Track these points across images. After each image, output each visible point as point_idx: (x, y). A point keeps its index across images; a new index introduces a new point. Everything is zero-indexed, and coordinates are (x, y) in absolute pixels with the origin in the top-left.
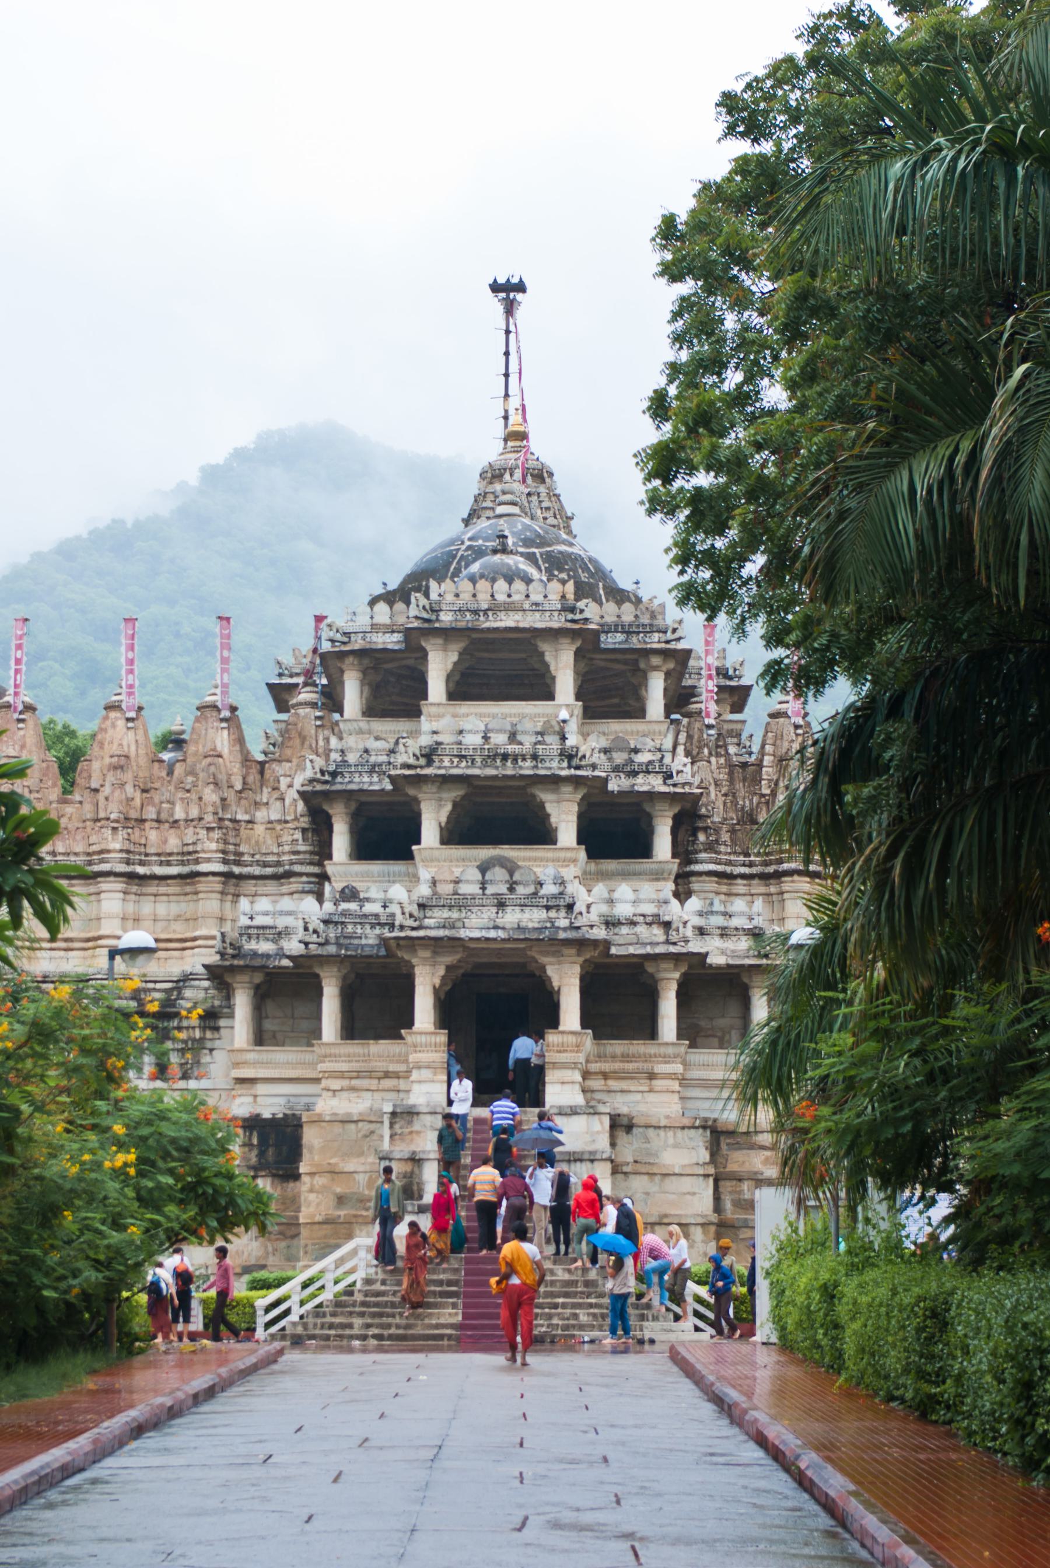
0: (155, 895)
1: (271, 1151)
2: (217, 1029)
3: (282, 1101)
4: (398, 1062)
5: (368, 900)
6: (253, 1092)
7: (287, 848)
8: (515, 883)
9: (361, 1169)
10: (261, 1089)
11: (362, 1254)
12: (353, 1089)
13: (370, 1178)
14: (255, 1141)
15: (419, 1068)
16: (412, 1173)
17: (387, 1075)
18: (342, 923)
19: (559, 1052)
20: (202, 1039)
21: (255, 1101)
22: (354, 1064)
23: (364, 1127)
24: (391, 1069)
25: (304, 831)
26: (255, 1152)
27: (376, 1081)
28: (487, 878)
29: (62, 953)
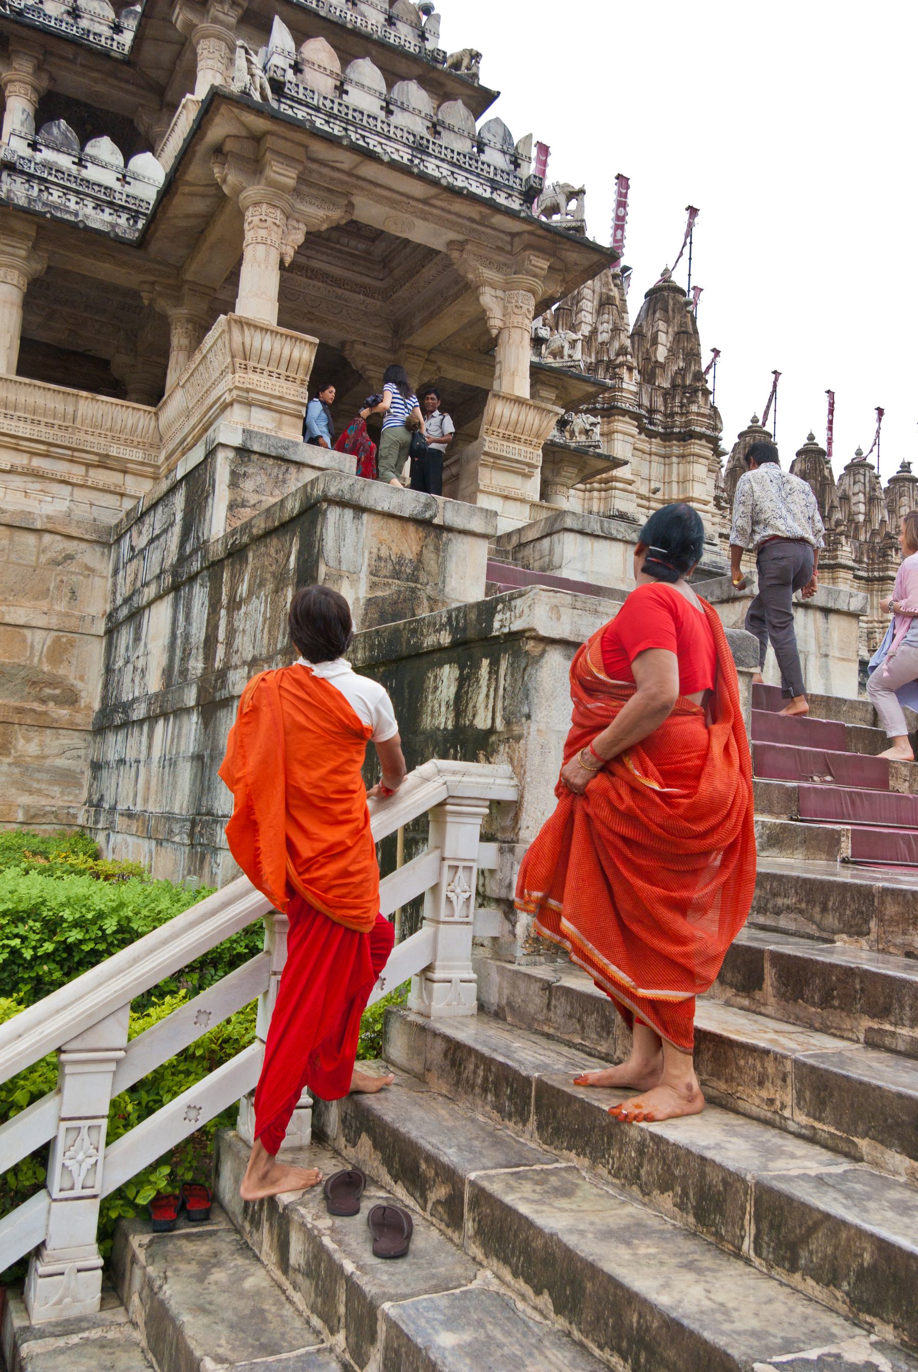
4: (128, 443)
5: (95, 161)
8: (442, 123)
9: (41, 621)
11: (463, 838)
12: (36, 475)
13: (57, 640)
15: (249, 404)
16: (419, 563)
17: (104, 462)
18: (43, 180)
19: (507, 438)
22: (42, 428)
23: (56, 545)
24: (114, 451)
27: (79, 470)
28: (395, 94)
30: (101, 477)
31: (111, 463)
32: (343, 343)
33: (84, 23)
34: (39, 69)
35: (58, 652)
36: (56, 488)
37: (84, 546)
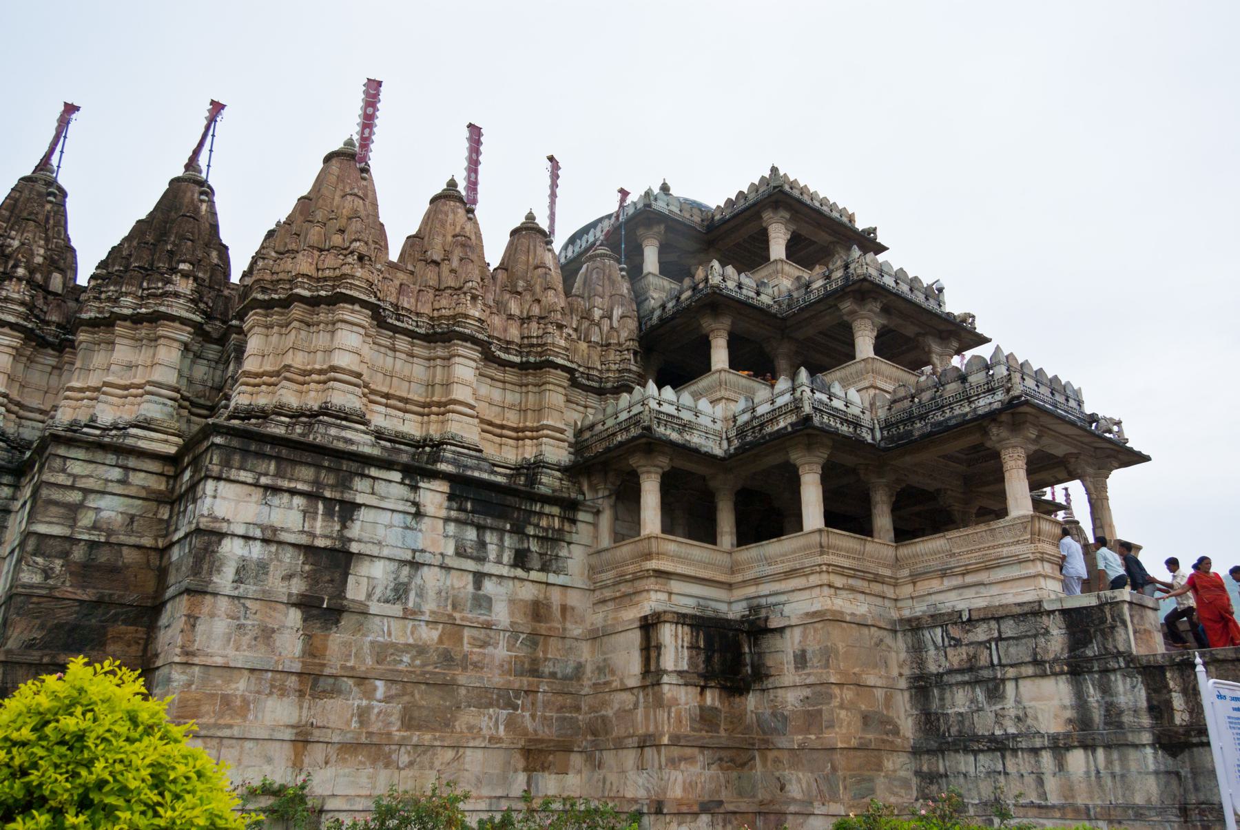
0: (492, 379)
1: (716, 656)
2: (574, 521)
3: (691, 602)
6: (667, 588)
7: (613, 367)
10: (675, 586)
12: (852, 589)
14: (702, 645)
17: (877, 579)
20: (561, 530)
21: (670, 599)
25: (635, 353)
26: (702, 657)
27: (865, 584)
29: (401, 414)
30: (876, 588)
31: (879, 579)
32: (938, 491)
33: (744, 291)
34: (733, 323)
35: (888, 700)
36: (861, 597)
37: (885, 633)
